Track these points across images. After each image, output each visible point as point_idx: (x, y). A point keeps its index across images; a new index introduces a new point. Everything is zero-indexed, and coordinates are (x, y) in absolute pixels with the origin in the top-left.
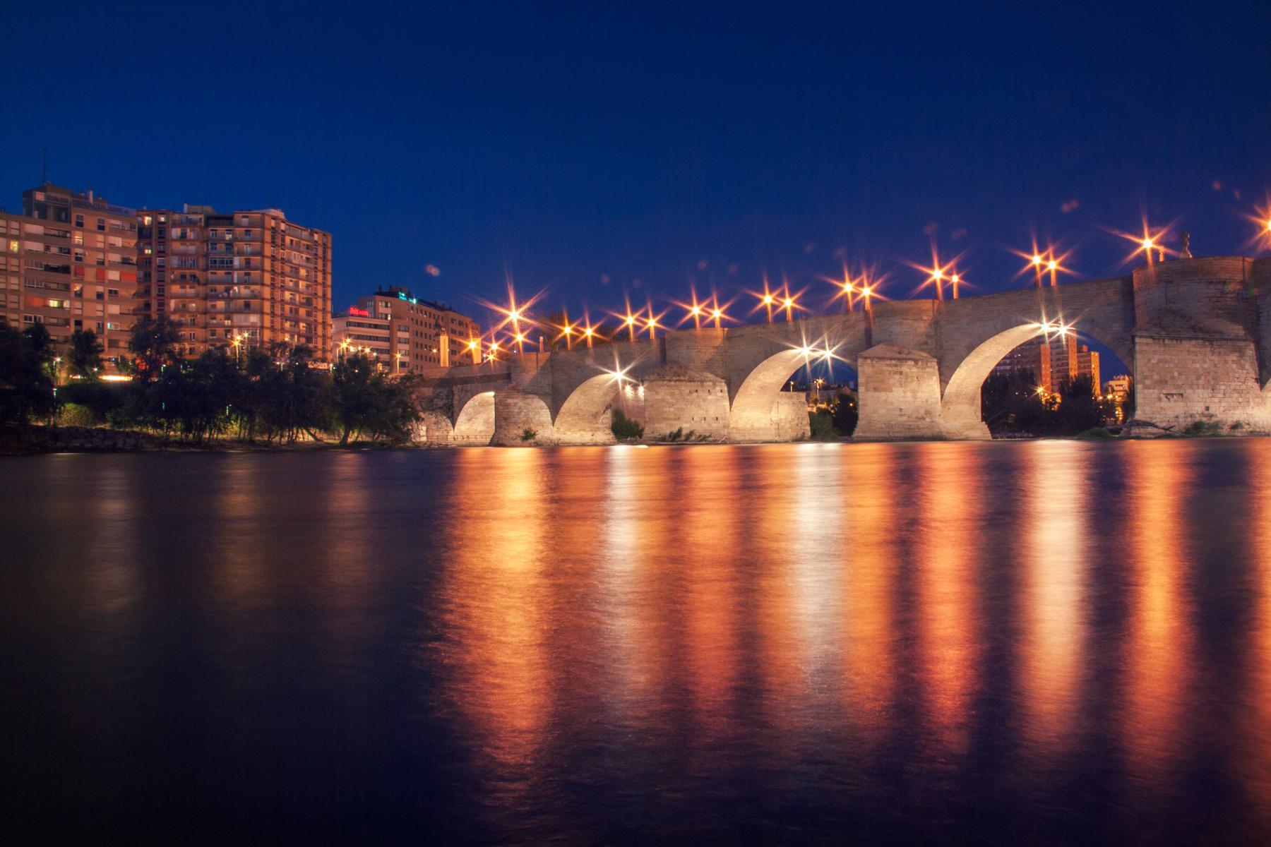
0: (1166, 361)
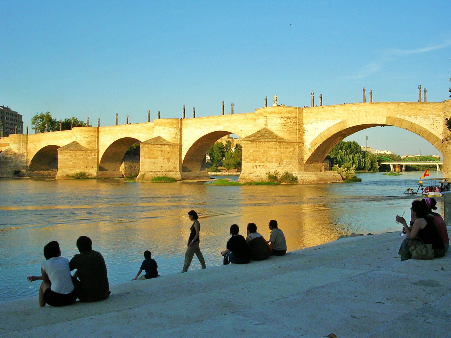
0: (257, 151)
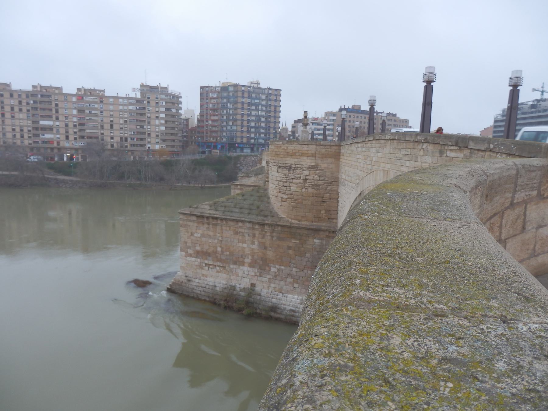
0: (210, 237)
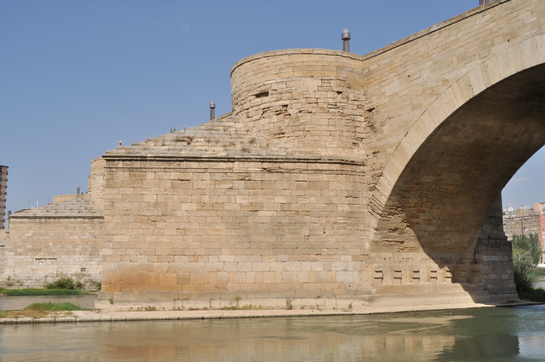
0: (41, 235)
